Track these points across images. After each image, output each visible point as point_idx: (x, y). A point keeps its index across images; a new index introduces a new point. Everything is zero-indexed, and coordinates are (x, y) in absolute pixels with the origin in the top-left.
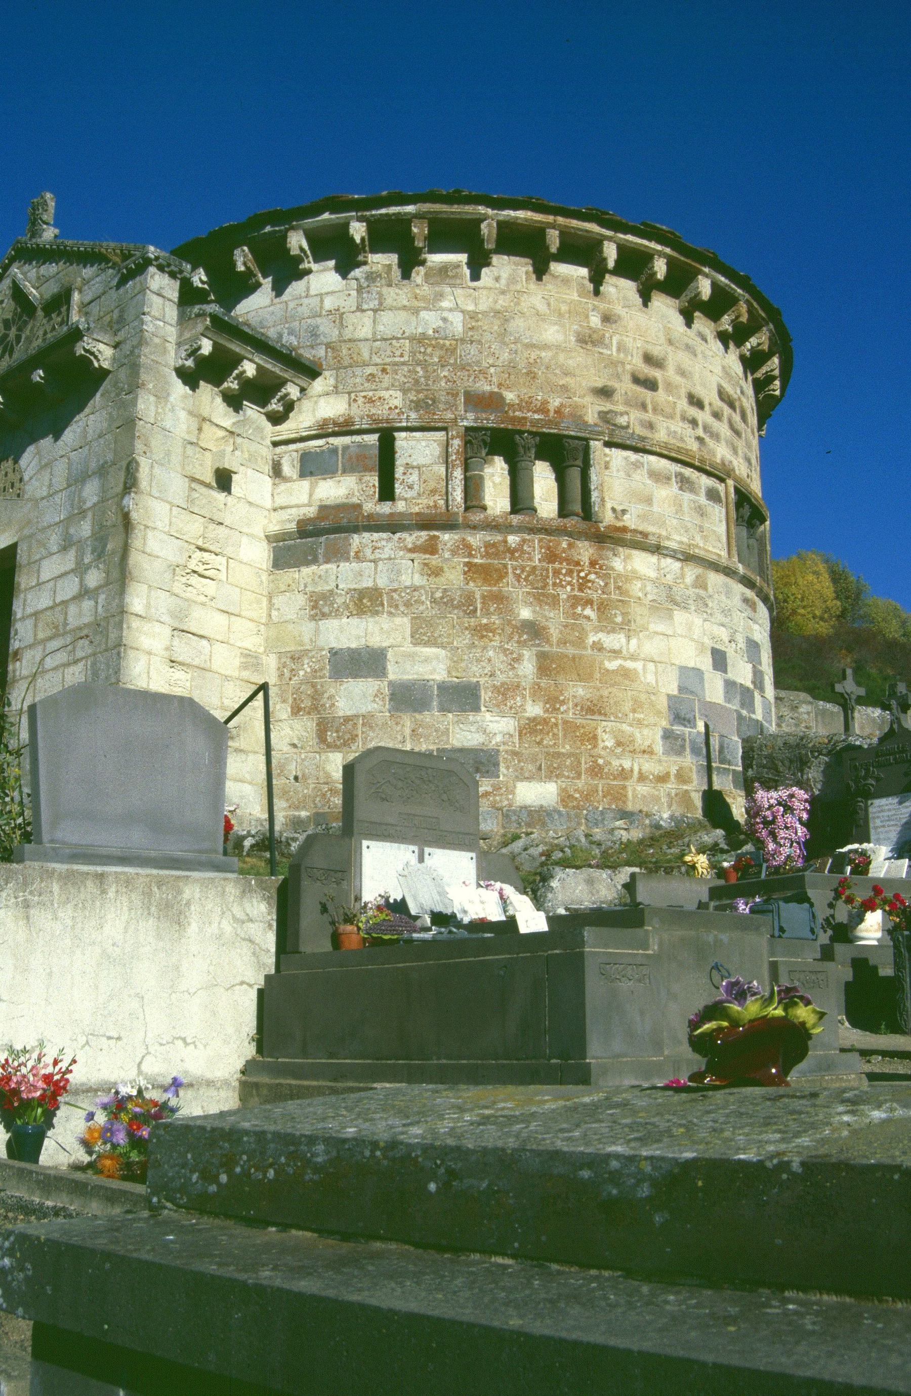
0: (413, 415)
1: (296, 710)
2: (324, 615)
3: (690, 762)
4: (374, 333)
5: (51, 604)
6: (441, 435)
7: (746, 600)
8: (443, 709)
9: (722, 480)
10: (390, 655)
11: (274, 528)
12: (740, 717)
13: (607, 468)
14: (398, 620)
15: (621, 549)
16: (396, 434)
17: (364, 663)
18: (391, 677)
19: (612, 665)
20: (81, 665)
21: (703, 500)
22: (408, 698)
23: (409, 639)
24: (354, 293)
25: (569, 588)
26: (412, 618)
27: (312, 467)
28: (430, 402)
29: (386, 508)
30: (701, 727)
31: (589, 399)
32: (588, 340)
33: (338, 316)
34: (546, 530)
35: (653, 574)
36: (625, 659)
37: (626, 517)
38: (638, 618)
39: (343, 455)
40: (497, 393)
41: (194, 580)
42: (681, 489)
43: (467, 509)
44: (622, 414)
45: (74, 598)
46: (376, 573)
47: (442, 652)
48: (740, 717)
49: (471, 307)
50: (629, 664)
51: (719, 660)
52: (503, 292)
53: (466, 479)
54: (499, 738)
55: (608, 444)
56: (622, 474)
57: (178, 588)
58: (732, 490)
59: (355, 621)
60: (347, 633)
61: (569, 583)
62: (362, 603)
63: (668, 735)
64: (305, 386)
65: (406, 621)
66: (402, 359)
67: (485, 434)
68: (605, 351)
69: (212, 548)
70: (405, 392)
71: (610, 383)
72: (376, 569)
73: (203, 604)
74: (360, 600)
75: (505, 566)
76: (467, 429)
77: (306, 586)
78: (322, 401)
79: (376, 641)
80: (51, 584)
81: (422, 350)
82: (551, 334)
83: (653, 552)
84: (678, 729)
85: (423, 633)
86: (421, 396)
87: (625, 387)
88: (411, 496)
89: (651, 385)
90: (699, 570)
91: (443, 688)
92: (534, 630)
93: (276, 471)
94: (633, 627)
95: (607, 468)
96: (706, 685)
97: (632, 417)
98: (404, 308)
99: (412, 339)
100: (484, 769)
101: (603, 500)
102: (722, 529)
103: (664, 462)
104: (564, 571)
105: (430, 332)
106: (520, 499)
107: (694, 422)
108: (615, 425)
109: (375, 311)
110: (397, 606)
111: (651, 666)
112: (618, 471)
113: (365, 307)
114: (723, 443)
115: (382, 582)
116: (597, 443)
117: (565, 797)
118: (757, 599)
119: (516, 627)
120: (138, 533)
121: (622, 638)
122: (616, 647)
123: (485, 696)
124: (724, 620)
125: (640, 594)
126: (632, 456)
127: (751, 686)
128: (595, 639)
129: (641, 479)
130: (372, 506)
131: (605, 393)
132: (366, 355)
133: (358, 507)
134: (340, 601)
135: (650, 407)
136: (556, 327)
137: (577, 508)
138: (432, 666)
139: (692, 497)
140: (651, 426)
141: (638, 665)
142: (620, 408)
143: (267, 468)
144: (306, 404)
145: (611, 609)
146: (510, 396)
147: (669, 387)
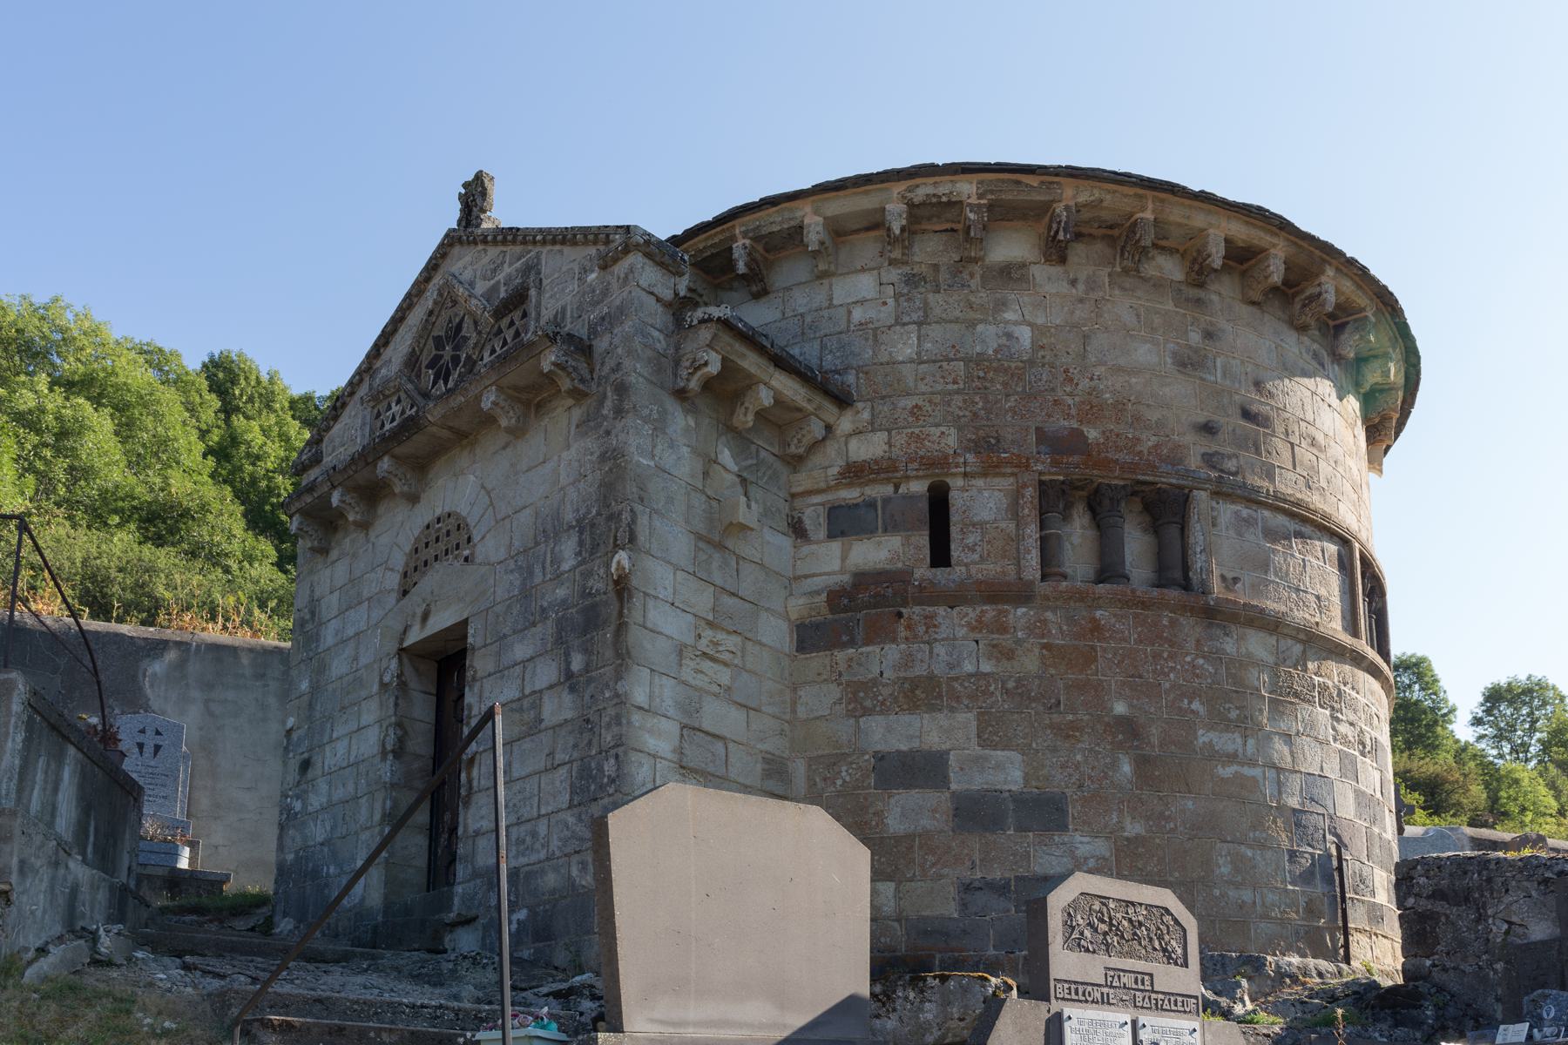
0: (970, 457)
2: (867, 712)
5: (517, 695)
8: (1022, 829)
14: (961, 717)
15: (1233, 627)
17: (920, 769)
18: (953, 786)
19: (1227, 771)
20: (563, 771)
22: (977, 813)
23: (975, 740)
24: (891, 301)
27: (844, 523)
29: (940, 574)
31: (1190, 438)
32: (1189, 363)
33: (874, 333)
39: (883, 509)
41: (707, 665)
43: (1044, 577)
44: (1230, 457)
45: (551, 687)
46: (931, 657)
47: (1016, 756)
49: (1040, 321)
52: (1081, 301)
56: (1232, 533)
57: (687, 674)
60: (893, 733)
68: (1208, 377)
70: (960, 429)
71: (1215, 418)
72: (931, 652)
73: (716, 695)
75: (1093, 648)
76: (1041, 473)
80: (518, 669)
81: (981, 374)
82: (1143, 354)
85: (991, 733)
91: (1019, 800)
92: (1129, 729)
93: (798, 530)
95: (1214, 525)
98: (956, 321)
99: (967, 360)
103: (1281, 519)
108: (1222, 471)
109: (920, 324)
110: (958, 699)
113: (906, 319)
119: (1108, 724)
120: (637, 601)
122: (1230, 748)
128: (1205, 739)
131: (1208, 429)
134: (886, 692)
138: (1009, 773)
141: (1256, 772)
142: (1229, 450)
143: (783, 526)
146: (1092, 434)
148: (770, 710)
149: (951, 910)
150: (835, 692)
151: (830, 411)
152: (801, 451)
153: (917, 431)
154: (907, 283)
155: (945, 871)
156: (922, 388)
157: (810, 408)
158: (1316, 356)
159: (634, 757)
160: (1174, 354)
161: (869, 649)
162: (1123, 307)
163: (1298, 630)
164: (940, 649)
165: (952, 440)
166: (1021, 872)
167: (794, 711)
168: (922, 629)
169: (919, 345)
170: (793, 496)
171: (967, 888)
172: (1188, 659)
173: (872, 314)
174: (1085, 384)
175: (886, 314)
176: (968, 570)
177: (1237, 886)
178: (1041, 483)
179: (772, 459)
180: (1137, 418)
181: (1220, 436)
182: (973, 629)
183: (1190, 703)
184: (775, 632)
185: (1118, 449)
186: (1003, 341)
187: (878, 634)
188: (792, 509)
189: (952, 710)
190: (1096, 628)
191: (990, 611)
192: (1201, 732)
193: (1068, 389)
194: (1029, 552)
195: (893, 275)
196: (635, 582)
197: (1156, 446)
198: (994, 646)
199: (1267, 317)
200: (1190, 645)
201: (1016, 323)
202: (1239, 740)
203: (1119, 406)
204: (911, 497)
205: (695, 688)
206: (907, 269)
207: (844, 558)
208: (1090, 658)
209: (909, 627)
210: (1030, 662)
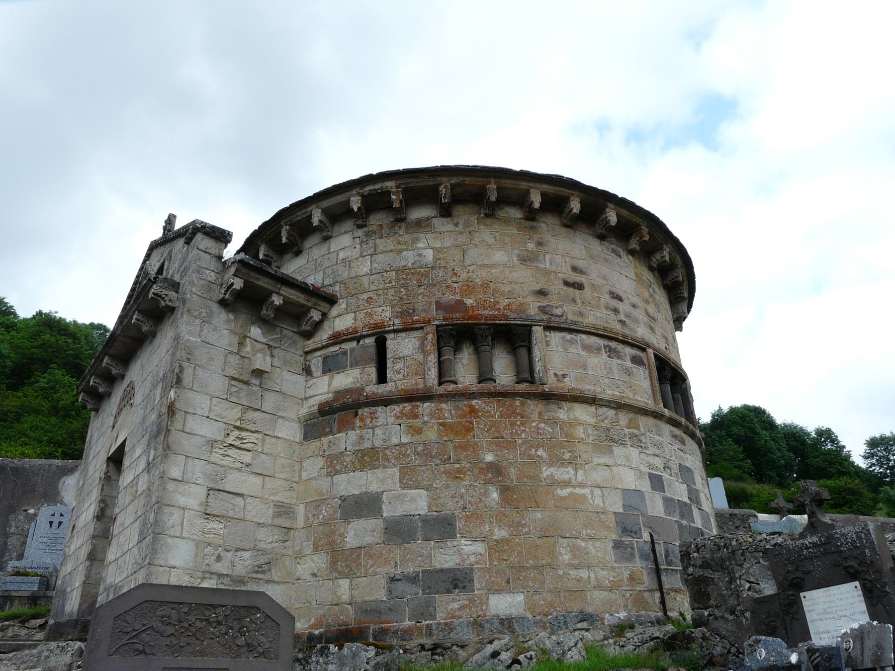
0: (397, 321)
1: (316, 549)
2: (338, 472)
3: (640, 565)
4: (371, 270)
6: (418, 334)
7: (675, 436)
8: (427, 539)
10: (384, 498)
11: (304, 411)
12: (681, 526)
13: (547, 345)
14: (390, 471)
15: (564, 403)
16: (387, 336)
18: (385, 515)
19: (564, 492)
21: (629, 364)
22: (399, 531)
24: (358, 246)
26: (401, 468)
27: (331, 366)
30: (646, 537)
31: (530, 299)
32: (526, 259)
33: (347, 263)
35: (592, 421)
36: (574, 487)
37: (566, 380)
38: (584, 455)
39: (351, 354)
42: (609, 357)
43: (440, 384)
44: (557, 307)
47: (423, 493)
48: (681, 526)
49: (438, 245)
50: (578, 491)
51: (657, 482)
52: (461, 233)
53: (440, 363)
54: (472, 559)
55: (548, 328)
56: (560, 349)
57: (215, 457)
58: (652, 356)
59: (358, 474)
60: (352, 484)
62: (364, 460)
63: (617, 545)
64: (326, 311)
65: (396, 470)
68: (540, 265)
69: (248, 427)
70: (392, 306)
71: (546, 287)
72: (373, 433)
73: (239, 470)
74: (362, 457)
75: (471, 423)
76: (437, 326)
78: (337, 321)
79: (374, 488)
84: (627, 539)
85: (408, 480)
87: (557, 288)
88: (399, 379)
89: (579, 287)
90: (631, 415)
91: (426, 521)
92: (496, 470)
94: (579, 461)
96: (648, 503)
97: (565, 308)
98: (391, 251)
99: (397, 270)
100: (461, 585)
101: (545, 367)
102: (646, 384)
103: (594, 340)
104: (518, 423)
105: (410, 265)
106: (485, 375)
108: (552, 315)
109: (371, 255)
110: (388, 460)
111: (597, 492)
112: (557, 346)
113: (365, 253)
117: (531, 606)
118: (684, 436)
119: (481, 468)
120: (179, 417)
121: (570, 470)
123: (459, 525)
124: (658, 452)
125: (583, 436)
126: (569, 336)
127: (688, 501)
129: (576, 350)
130: (373, 389)
131: (542, 293)
133: (361, 390)
134: (348, 459)
135: (579, 301)
136: (502, 252)
137: (526, 375)
138: (418, 503)
139: (620, 362)
140: (581, 314)
141: (586, 491)
142: (555, 303)
144: (326, 325)
145: (563, 451)
146: (469, 301)
147: (594, 287)
148: (282, 475)
149: (382, 595)
150: (321, 462)
151: (324, 306)
152: (308, 328)
154: (366, 236)
155: (379, 570)
156: (373, 288)
158: (614, 251)
159: (166, 510)
160: (519, 255)
161: (340, 435)
162: (486, 234)
163: (609, 402)
164: (378, 431)
165: (388, 314)
166: (426, 567)
167: (300, 476)
168: (369, 420)
170: (307, 353)
171: (393, 580)
172: (534, 424)
173: (349, 254)
174: (464, 275)
175: (356, 253)
176: (396, 384)
177: (576, 567)
178: (437, 331)
179: (292, 334)
180: (496, 291)
181: (550, 297)
182: (398, 418)
183: (536, 451)
184: (290, 431)
185: (484, 308)
187: (345, 426)
188: (306, 361)
189: (385, 467)
190: (473, 411)
191: (408, 406)
192: (544, 469)
193: (454, 279)
194: (429, 370)
195: (360, 233)
196: (177, 405)
197: (508, 305)
198: (410, 427)
199: (577, 233)
200: (535, 416)
201: (424, 249)
202: (572, 472)
203: (485, 286)
204: (365, 347)
205: (222, 466)
206: (366, 229)
207: (329, 385)
208: (469, 429)
209: (362, 420)
210: (431, 434)
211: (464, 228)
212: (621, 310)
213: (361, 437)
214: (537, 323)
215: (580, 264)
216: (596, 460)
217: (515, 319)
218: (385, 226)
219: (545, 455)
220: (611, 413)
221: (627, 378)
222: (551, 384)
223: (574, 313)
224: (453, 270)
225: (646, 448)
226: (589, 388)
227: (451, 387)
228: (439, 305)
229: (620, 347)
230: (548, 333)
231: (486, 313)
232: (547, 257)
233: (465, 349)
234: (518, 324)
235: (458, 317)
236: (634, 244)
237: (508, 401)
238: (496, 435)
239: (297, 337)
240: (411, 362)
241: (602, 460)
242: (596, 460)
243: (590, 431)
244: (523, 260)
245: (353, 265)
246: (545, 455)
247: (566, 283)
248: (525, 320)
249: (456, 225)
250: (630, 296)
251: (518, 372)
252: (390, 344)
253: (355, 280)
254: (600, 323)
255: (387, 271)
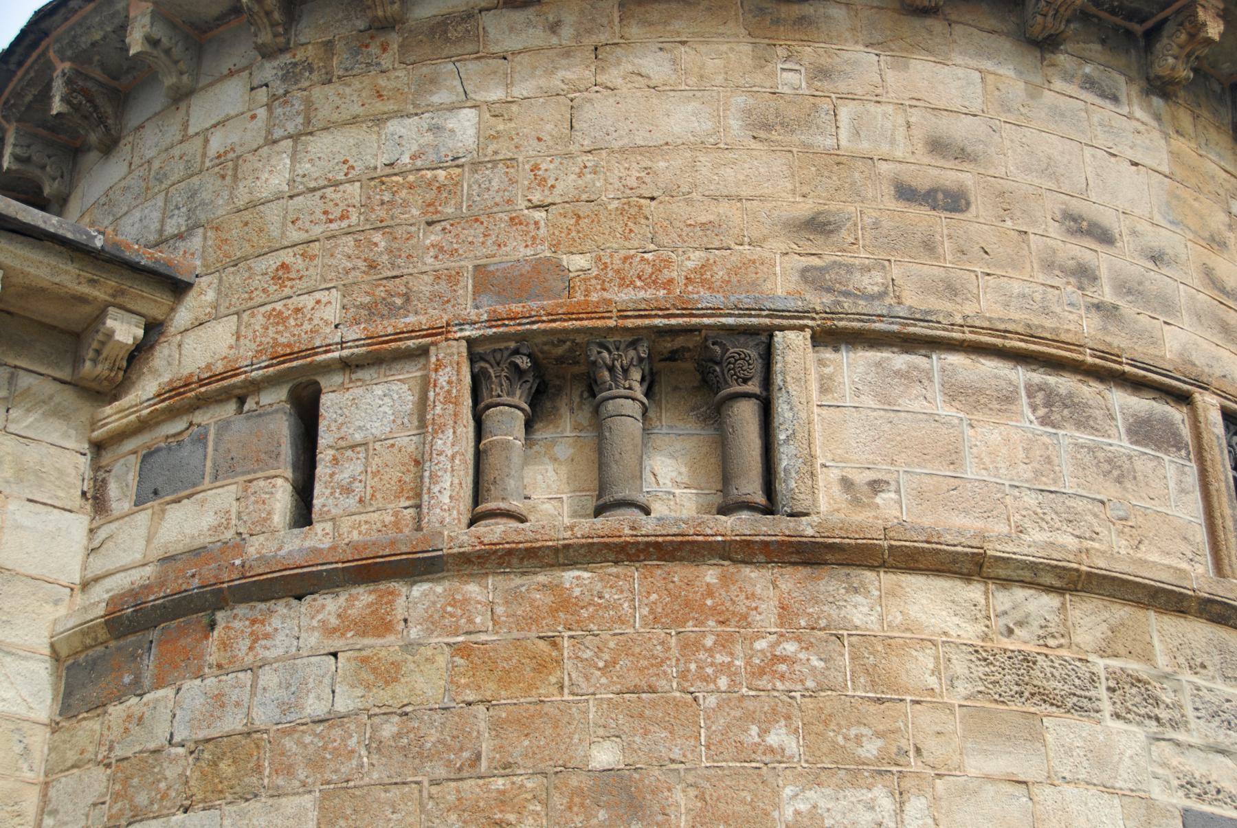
9: (1183, 399)
14: (289, 804)
15: (869, 575)
16: (324, 382)
21: (1121, 444)
24: (262, 113)
25: (723, 682)
28: (399, 301)
34: (657, 545)
35: (970, 632)
39: (216, 444)
40: (548, 259)
42: (1044, 421)
46: (253, 694)
52: (567, 53)
53: (479, 455)
55: (830, 337)
56: (868, 401)
58: (1216, 417)
61: (726, 668)
64: (156, 312)
66: (344, 224)
67: (516, 352)
70: (346, 290)
71: (833, 206)
72: (254, 686)
76: (470, 342)
77: (111, 749)
78: (190, 339)
81: (387, 197)
83: (967, 577)
86: (380, 292)
90: (1121, 612)
94: (914, 764)
98: (354, 121)
103: (989, 367)
104: (709, 641)
105: (406, 159)
107: (1084, 274)
108: (847, 294)
109: (295, 137)
110: (289, 771)
112: (857, 392)
113: (279, 133)
114: (1186, 320)
115: (262, 717)
116: (791, 335)
119: (578, 791)
125: (932, 681)
126: (900, 360)
131: (817, 226)
132: (275, 231)
134: (171, 772)
137: (752, 488)
139: (1084, 437)
140: (952, 290)
142: (862, 256)
147: (1005, 203)
151: (154, 302)
153: (279, 306)
154: (284, 79)
156: (295, 235)
157: (99, 294)
158: (1089, 84)
160: (748, 112)
161: (161, 693)
163: (1034, 567)
164: (268, 678)
165: (332, 313)
168: (244, 644)
169: (292, 170)
172: (761, 645)
173: (234, 138)
174: (567, 184)
175: (253, 132)
176: (336, 527)
178: (473, 358)
179: (50, 388)
181: (845, 236)
182: (330, 632)
183: (764, 732)
185: (624, 283)
186: (429, 137)
189: (278, 794)
190: (564, 603)
191: (363, 597)
192: (788, 791)
193: (537, 198)
195: (268, 71)
198: (364, 660)
199: (958, 30)
200: (766, 617)
202: (886, 804)
203: (632, 209)
206: (286, 58)
207: (149, 541)
210: (426, 682)
211: (578, 36)
212: (1104, 272)
213: (219, 700)
214: (793, 318)
215: (960, 129)
216: (976, 765)
217: (716, 311)
218: (339, 46)
219: (792, 745)
220: (1041, 605)
221: (1108, 490)
222: (825, 506)
223: (927, 288)
224: (535, 168)
225: (1174, 724)
226: (959, 527)
227: (495, 531)
228: (484, 279)
229: (1089, 391)
230: (828, 354)
231: (624, 296)
232: (845, 113)
233: (564, 410)
234: (724, 328)
235: (538, 312)
236: (1171, 60)
237: (679, 572)
238: (633, 679)
239: (66, 397)
240: (388, 457)
241: (1001, 764)
242: (976, 765)
243: (959, 666)
244: (762, 126)
245: (245, 168)
246: (792, 745)
247: (906, 193)
248: (747, 312)
249: (554, 28)
250: (1143, 226)
251: (726, 477)
252: (328, 402)
253: (247, 215)
254: (1017, 317)
255: (336, 184)
